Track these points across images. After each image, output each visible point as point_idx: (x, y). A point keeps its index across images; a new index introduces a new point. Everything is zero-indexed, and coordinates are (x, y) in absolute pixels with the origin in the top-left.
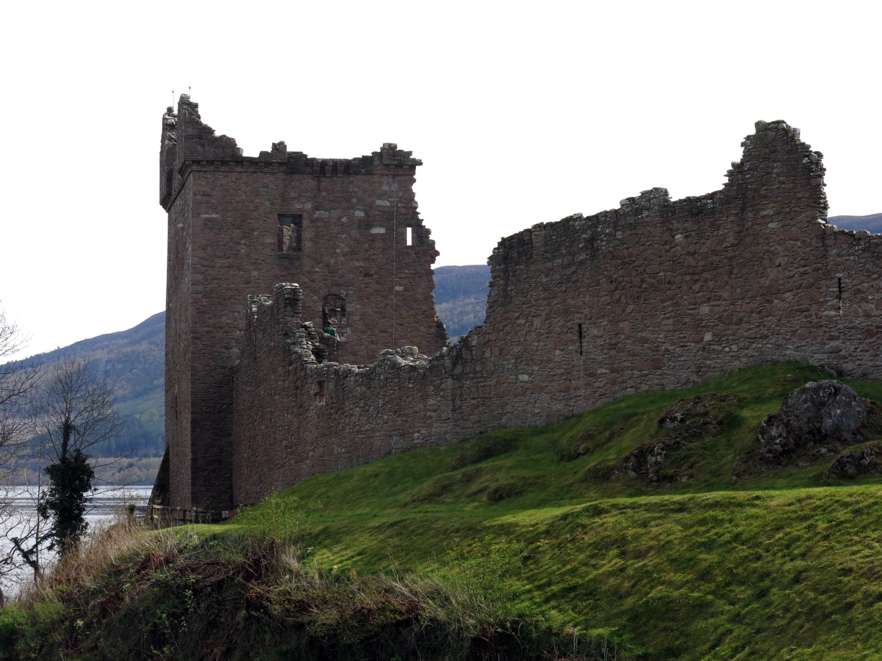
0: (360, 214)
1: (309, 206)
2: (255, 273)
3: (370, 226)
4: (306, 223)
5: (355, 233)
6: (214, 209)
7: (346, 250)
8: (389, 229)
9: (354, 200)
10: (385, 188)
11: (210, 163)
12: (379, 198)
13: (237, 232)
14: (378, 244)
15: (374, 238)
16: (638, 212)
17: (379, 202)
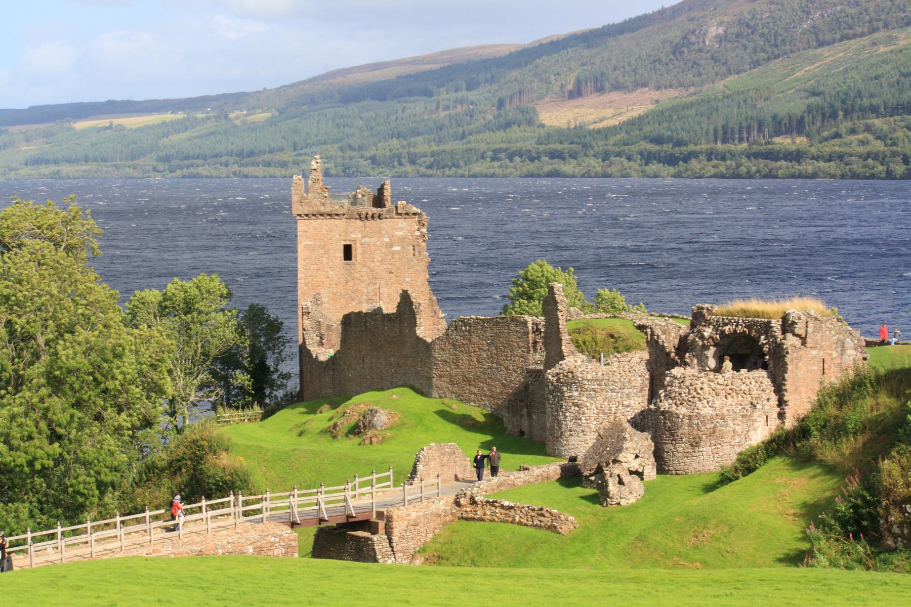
0: (387, 240)
1: (359, 236)
2: (331, 273)
3: (391, 246)
4: (358, 245)
5: (384, 250)
6: (309, 239)
7: (380, 259)
8: (403, 247)
9: (384, 232)
10: (400, 225)
11: (307, 215)
12: (398, 230)
13: (321, 251)
14: (396, 256)
15: (394, 253)
16: (376, 314)
17: (397, 233)
